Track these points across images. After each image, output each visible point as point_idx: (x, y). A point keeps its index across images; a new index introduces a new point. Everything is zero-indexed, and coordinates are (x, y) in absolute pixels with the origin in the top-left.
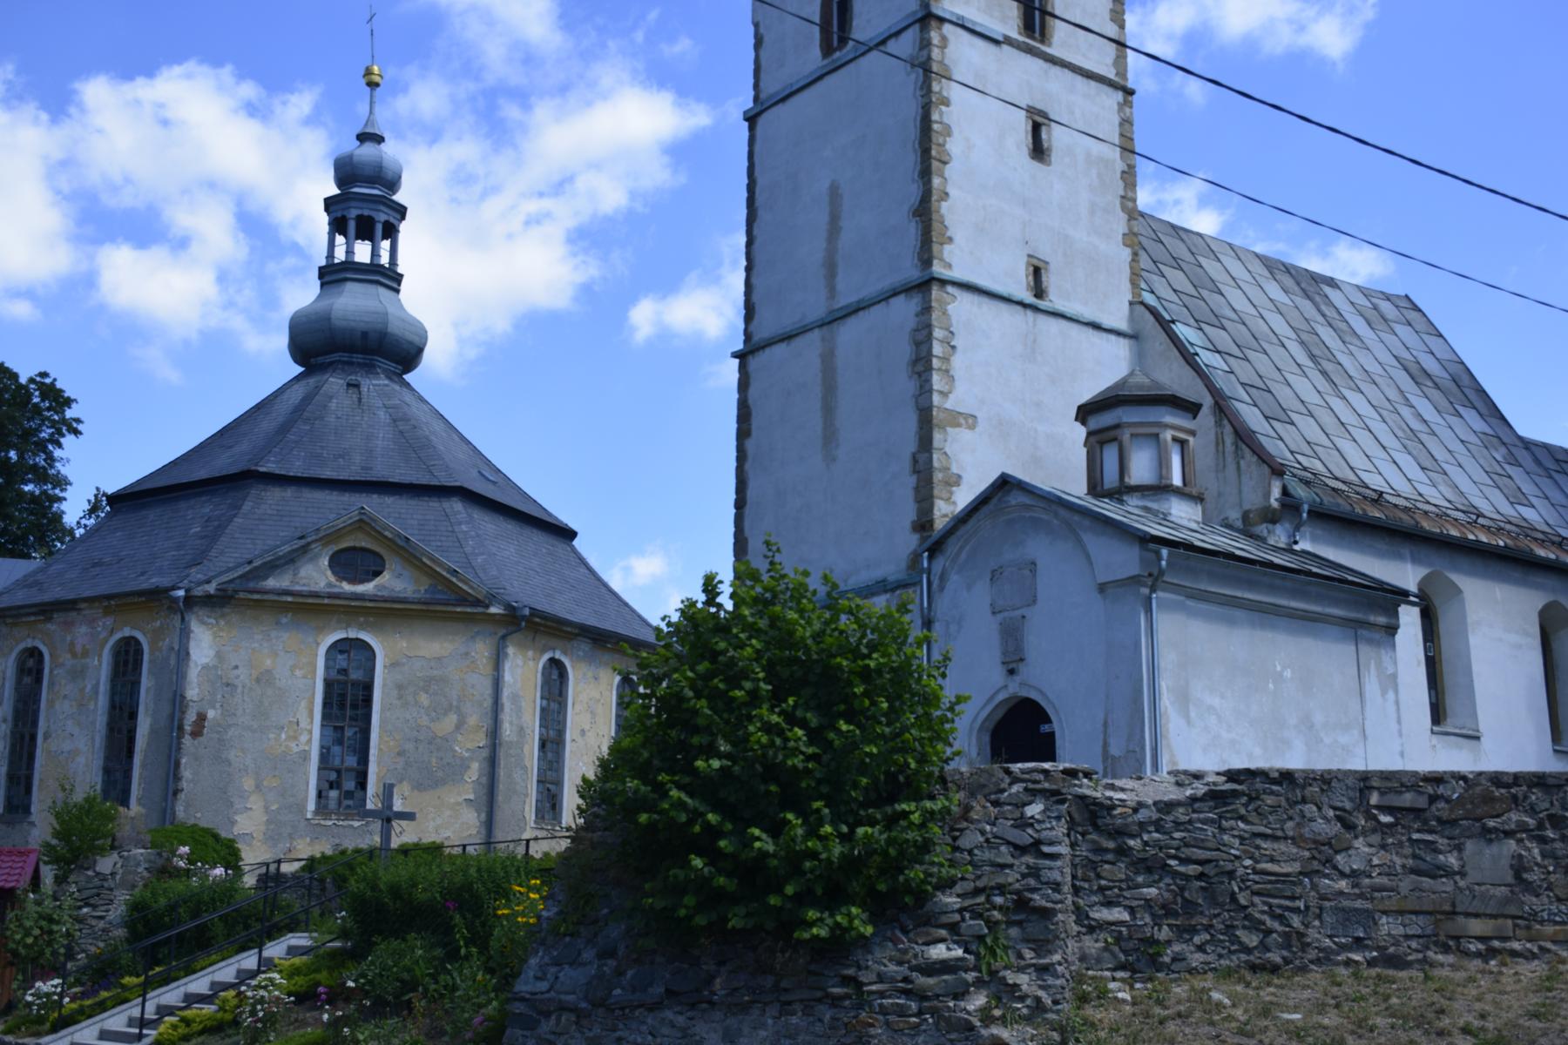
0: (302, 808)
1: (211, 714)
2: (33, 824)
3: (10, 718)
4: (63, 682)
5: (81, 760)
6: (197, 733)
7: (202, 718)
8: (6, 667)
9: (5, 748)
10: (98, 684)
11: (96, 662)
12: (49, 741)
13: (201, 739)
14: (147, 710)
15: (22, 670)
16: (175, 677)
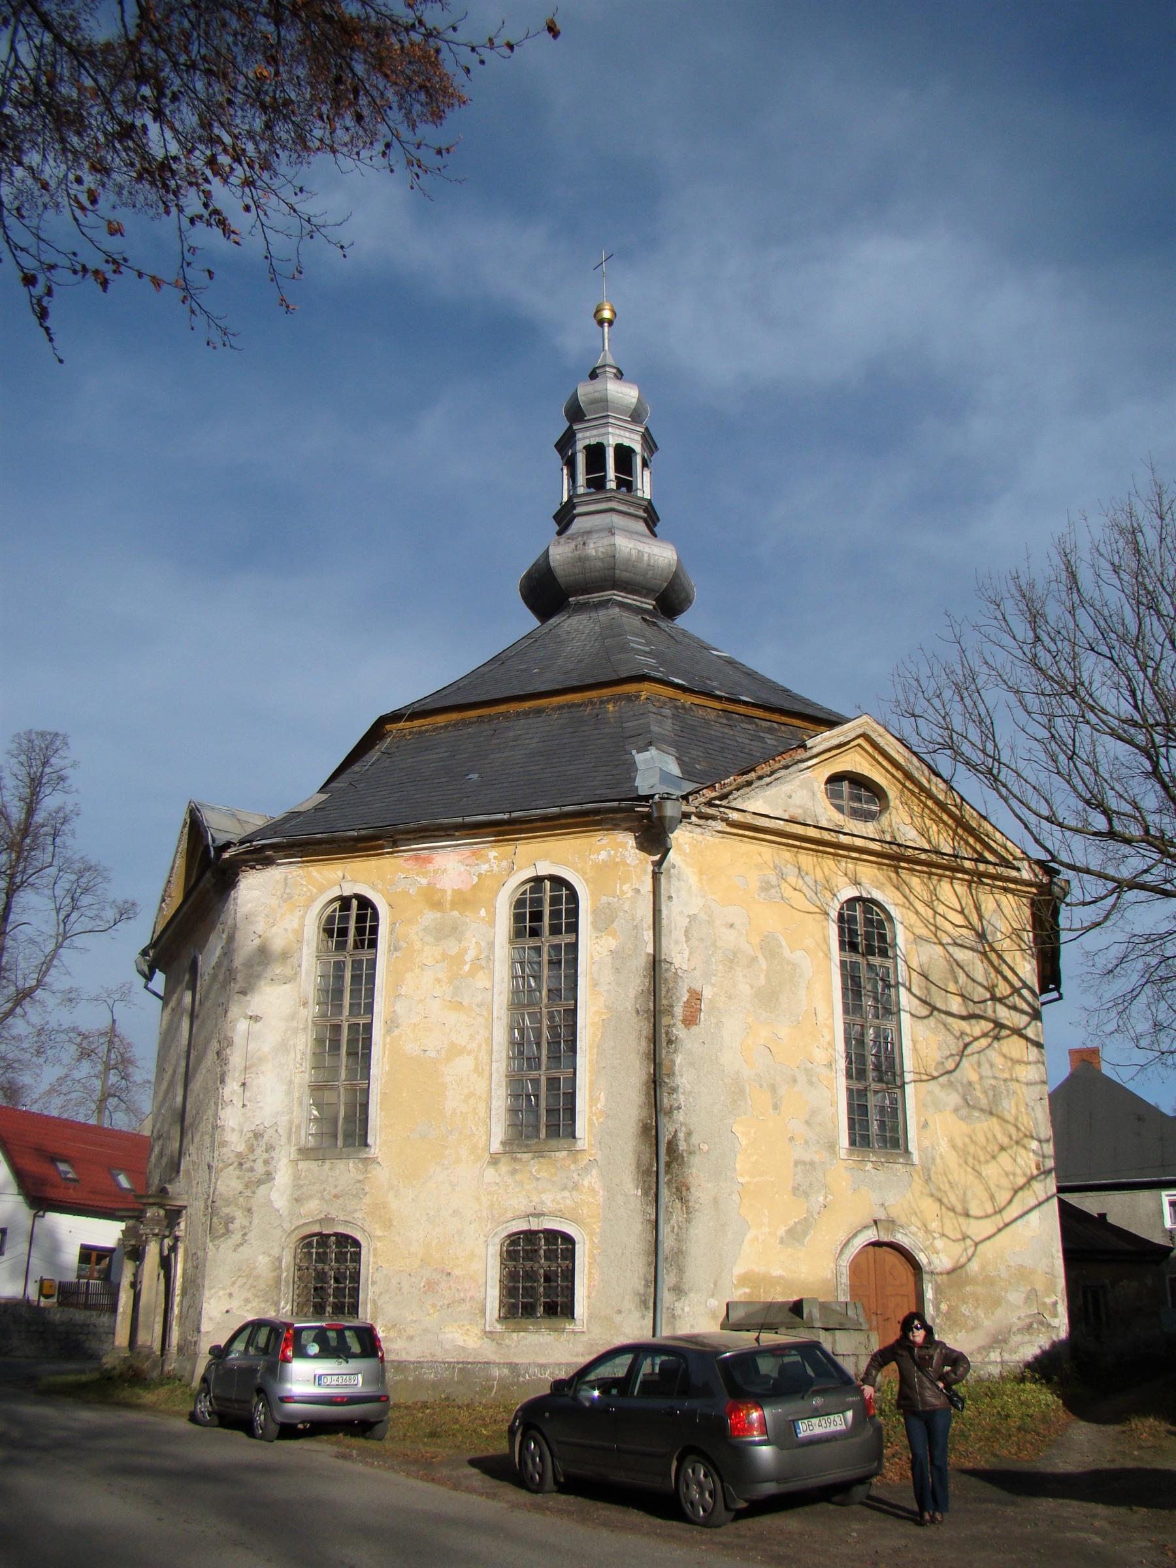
0: (832, 1147)
1: (707, 993)
2: (374, 1160)
3: (311, 1001)
4: (418, 945)
5: (464, 1065)
6: (691, 1020)
7: (696, 997)
8: (302, 925)
9: (307, 1045)
10: (491, 945)
11: (483, 912)
12: (397, 1032)
13: (694, 1029)
14: (595, 984)
15: (333, 930)
16: (648, 935)
